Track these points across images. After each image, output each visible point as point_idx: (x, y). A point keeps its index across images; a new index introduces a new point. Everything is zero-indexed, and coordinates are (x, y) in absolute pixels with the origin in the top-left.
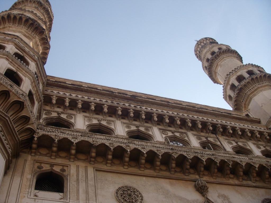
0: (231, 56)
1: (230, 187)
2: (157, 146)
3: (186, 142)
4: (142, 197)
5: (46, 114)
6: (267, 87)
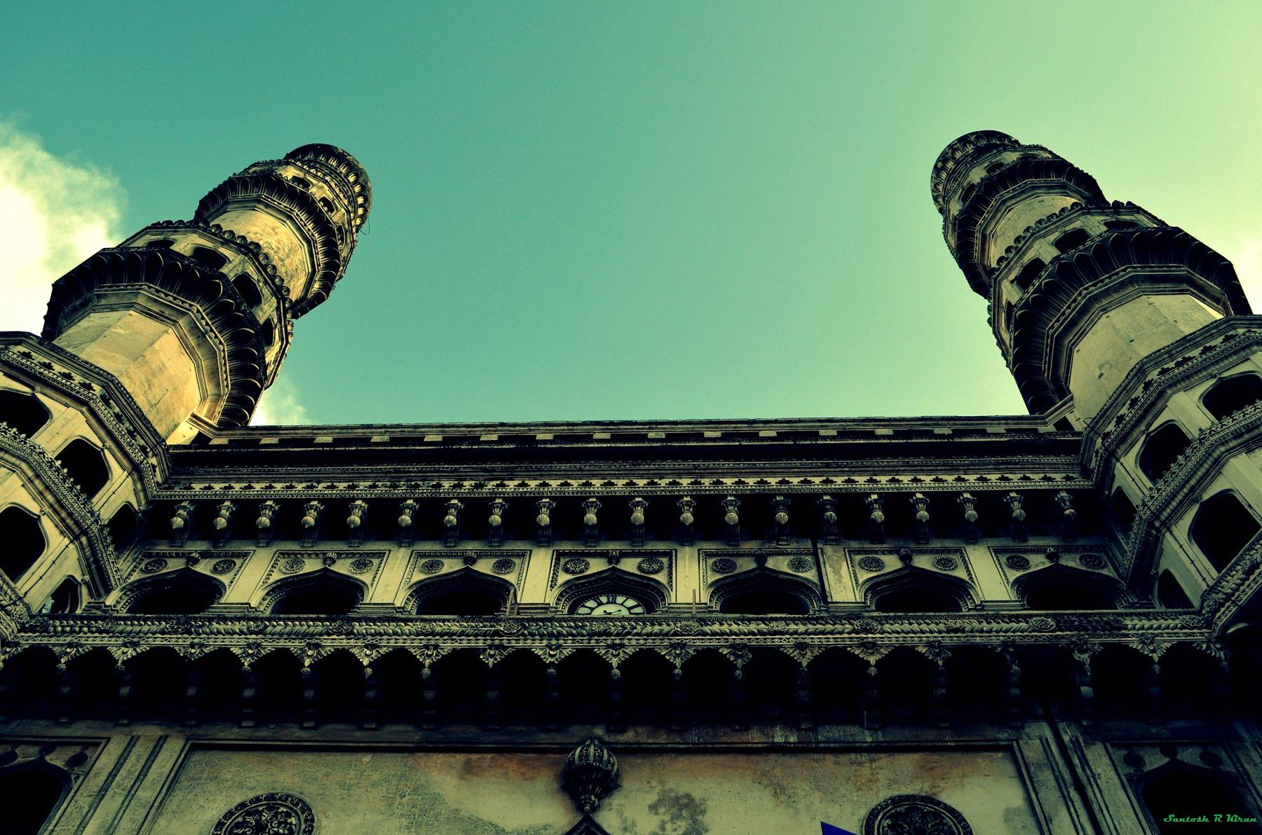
0: (1034, 188)
1: (742, 759)
2: (438, 629)
3: (654, 588)
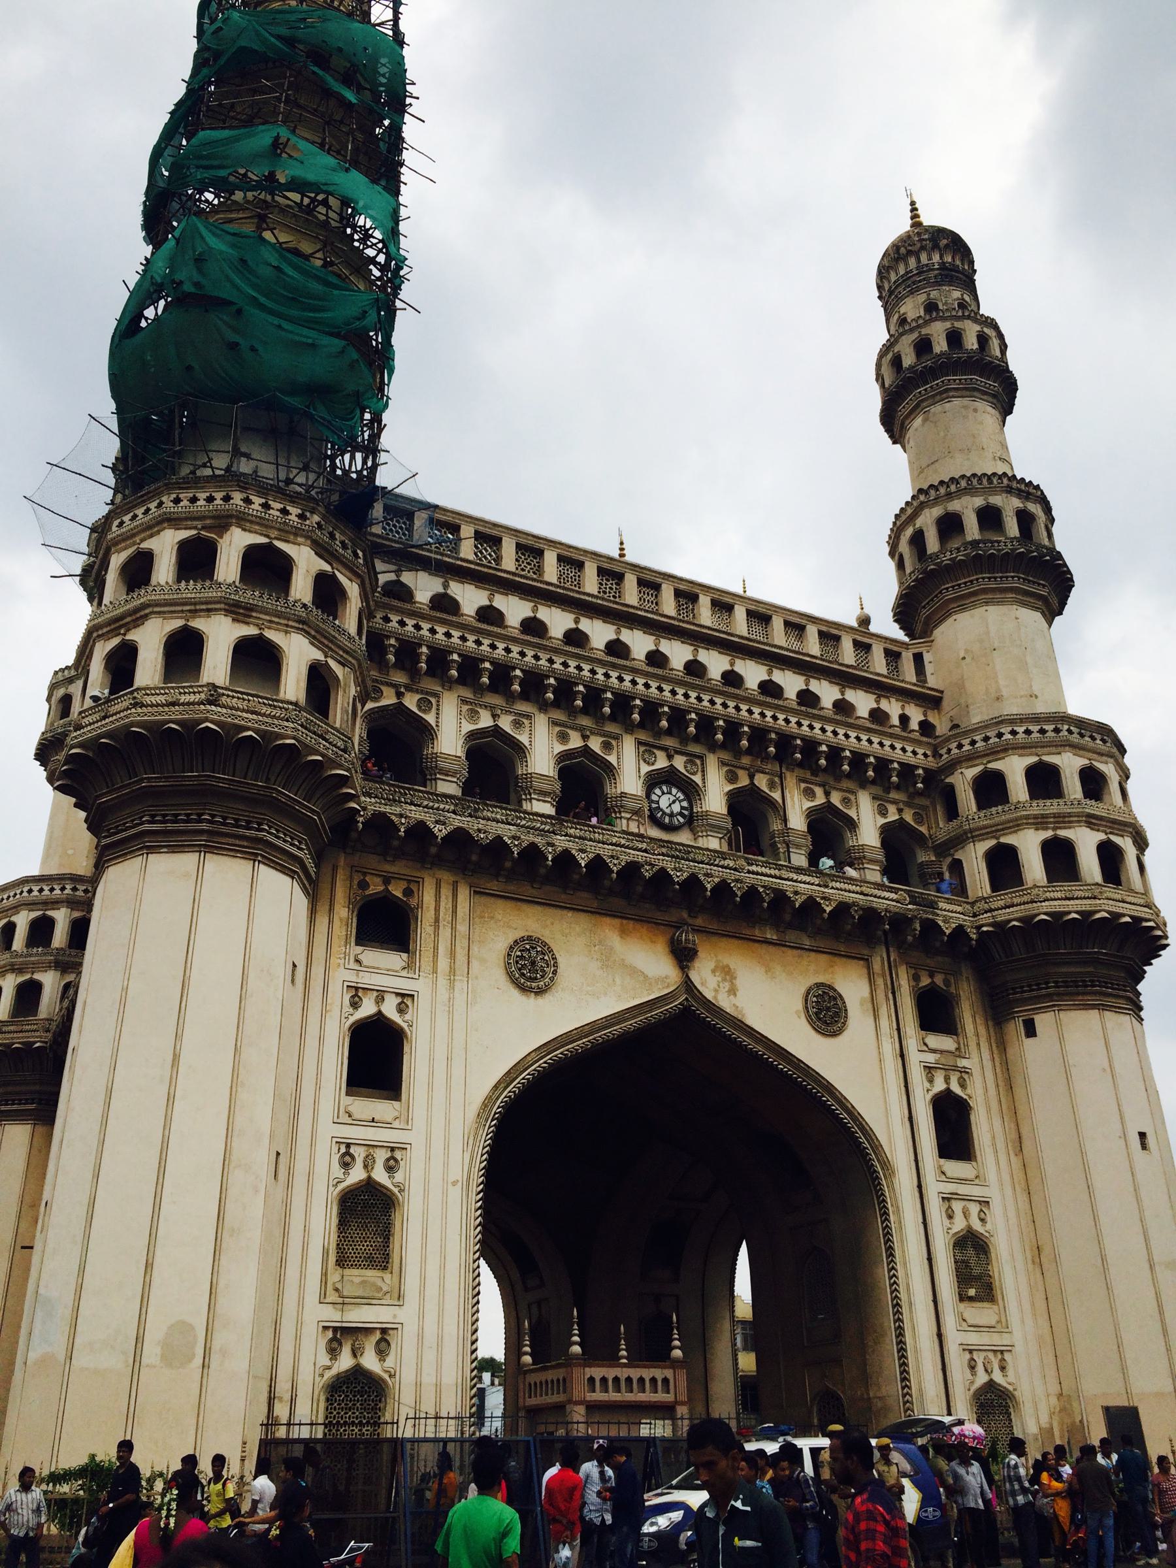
1: (751, 944)
4: (556, 965)
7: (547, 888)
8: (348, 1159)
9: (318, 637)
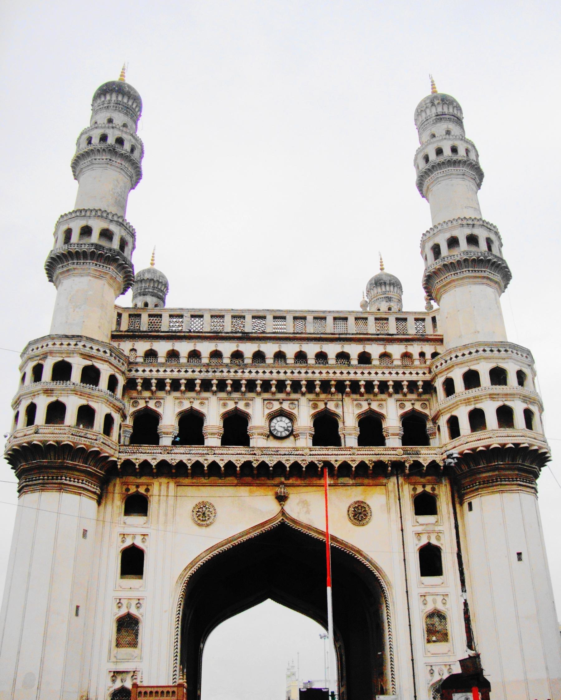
5: (133, 406)
6: (465, 280)
7: (212, 478)
8: (120, 605)
9: (83, 394)
